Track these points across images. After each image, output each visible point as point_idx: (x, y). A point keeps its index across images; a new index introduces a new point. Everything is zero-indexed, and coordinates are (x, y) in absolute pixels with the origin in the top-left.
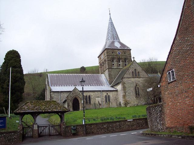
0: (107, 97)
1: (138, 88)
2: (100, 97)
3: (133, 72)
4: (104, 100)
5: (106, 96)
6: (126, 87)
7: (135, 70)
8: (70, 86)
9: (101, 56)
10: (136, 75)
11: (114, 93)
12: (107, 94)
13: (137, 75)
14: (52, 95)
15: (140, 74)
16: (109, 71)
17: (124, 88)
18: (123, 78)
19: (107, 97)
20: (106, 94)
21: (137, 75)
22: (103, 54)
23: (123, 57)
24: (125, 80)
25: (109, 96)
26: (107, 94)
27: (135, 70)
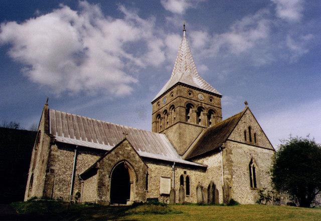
0: (185, 180)
1: (254, 168)
2: (169, 176)
3: (245, 132)
4: (178, 186)
5: (182, 177)
6: (232, 162)
7: (250, 128)
8: (96, 143)
9: (161, 100)
10: (251, 140)
11: (198, 173)
12: (185, 172)
13: (253, 140)
14: (52, 153)
15: (258, 138)
16: (180, 128)
17: (229, 163)
18: (227, 140)
19: (185, 180)
20: (182, 173)
21: (253, 140)
22: (169, 93)
23: (207, 106)
24: (230, 145)
25: (188, 178)
26: (185, 172)
27: (250, 128)
